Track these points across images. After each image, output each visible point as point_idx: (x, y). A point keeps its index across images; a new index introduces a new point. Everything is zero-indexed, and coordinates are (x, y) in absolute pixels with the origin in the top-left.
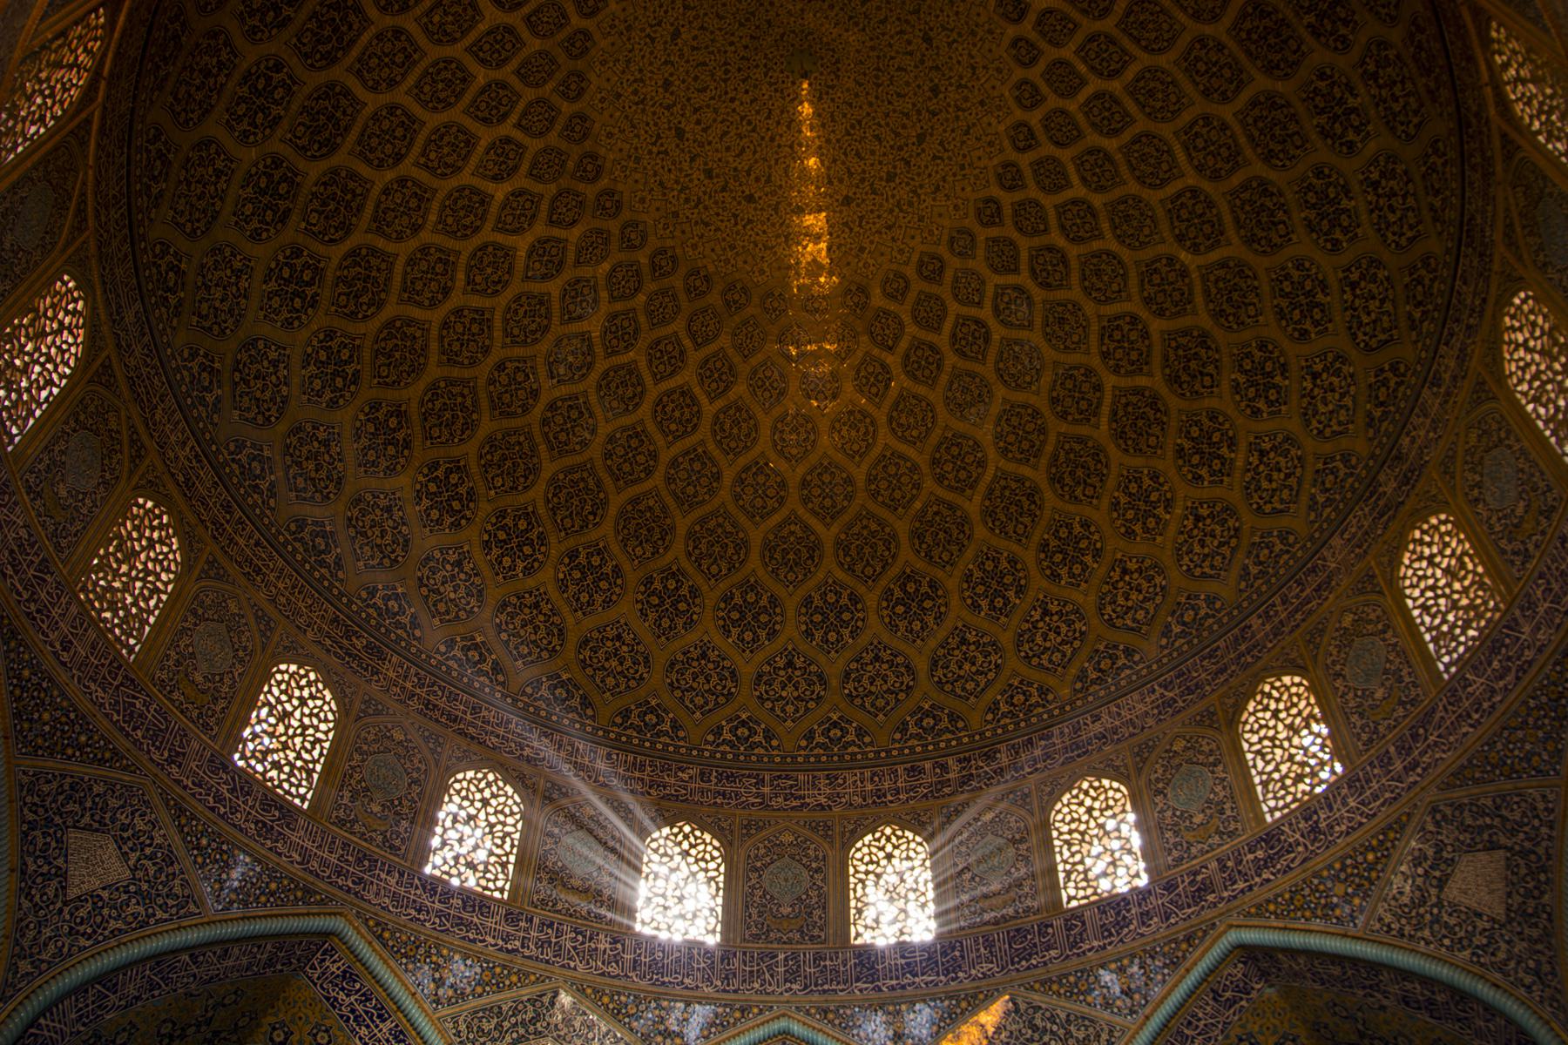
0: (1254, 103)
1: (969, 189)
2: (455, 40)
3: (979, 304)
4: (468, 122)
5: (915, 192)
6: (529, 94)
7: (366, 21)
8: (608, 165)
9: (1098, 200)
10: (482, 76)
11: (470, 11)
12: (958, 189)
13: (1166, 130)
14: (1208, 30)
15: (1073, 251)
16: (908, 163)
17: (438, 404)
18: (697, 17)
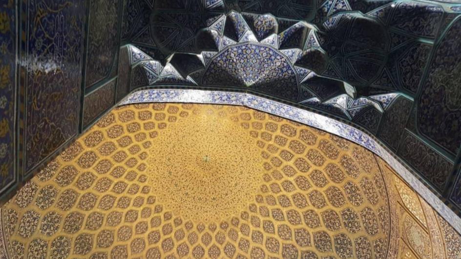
0: (75, 201)
1: (160, 138)
2: (286, 226)
3: (156, 114)
4: (292, 202)
5: (177, 134)
6: (276, 196)
7: (303, 253)
8: (262, 164)
9: (120, 149)
10: (285, 210)
11: (280, 230)
12: (163, 138)
13: (100, 176)
14: (91, 211)
15: (126, 133)
16: (178, 140)
17: (332, 154)
18: (230, 187)
